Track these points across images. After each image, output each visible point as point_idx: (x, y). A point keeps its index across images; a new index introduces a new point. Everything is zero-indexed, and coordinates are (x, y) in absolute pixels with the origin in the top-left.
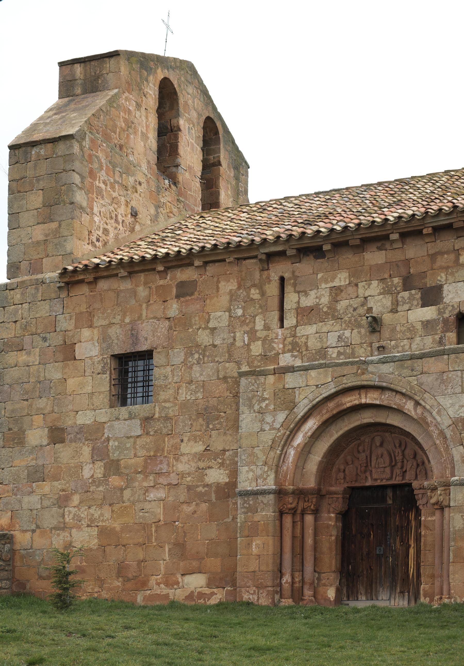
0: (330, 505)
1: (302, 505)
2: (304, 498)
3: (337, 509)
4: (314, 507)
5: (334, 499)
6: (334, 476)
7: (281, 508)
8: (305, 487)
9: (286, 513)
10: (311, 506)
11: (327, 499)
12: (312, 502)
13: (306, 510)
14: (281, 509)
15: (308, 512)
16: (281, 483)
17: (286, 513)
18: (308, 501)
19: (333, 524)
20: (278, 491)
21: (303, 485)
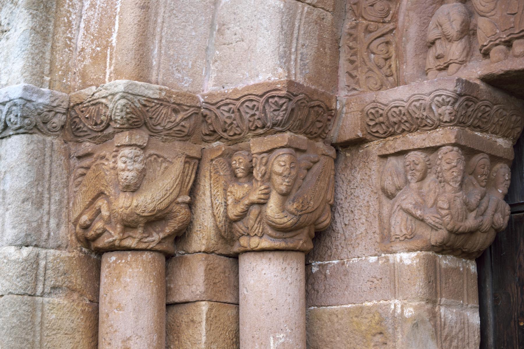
0: (391, 196)
1: (220, 200)
2: (228, 156)
3: (430, 219)
4: (283, 209)
5: (412, 156)
6: (413, 31)
7: (85, 218)
8: (229, 89)
9: (112, 249)
10: (262, 204)
11: (375, 165)
12: (268, 178)
13: (240, 227)
14: (86, 228)
15: (255, 242)
16: (83, 75)
17: (112, 249)
18: (249, 173)
19: (409, 312)
20: (58, 120)
21: (218, 81)
